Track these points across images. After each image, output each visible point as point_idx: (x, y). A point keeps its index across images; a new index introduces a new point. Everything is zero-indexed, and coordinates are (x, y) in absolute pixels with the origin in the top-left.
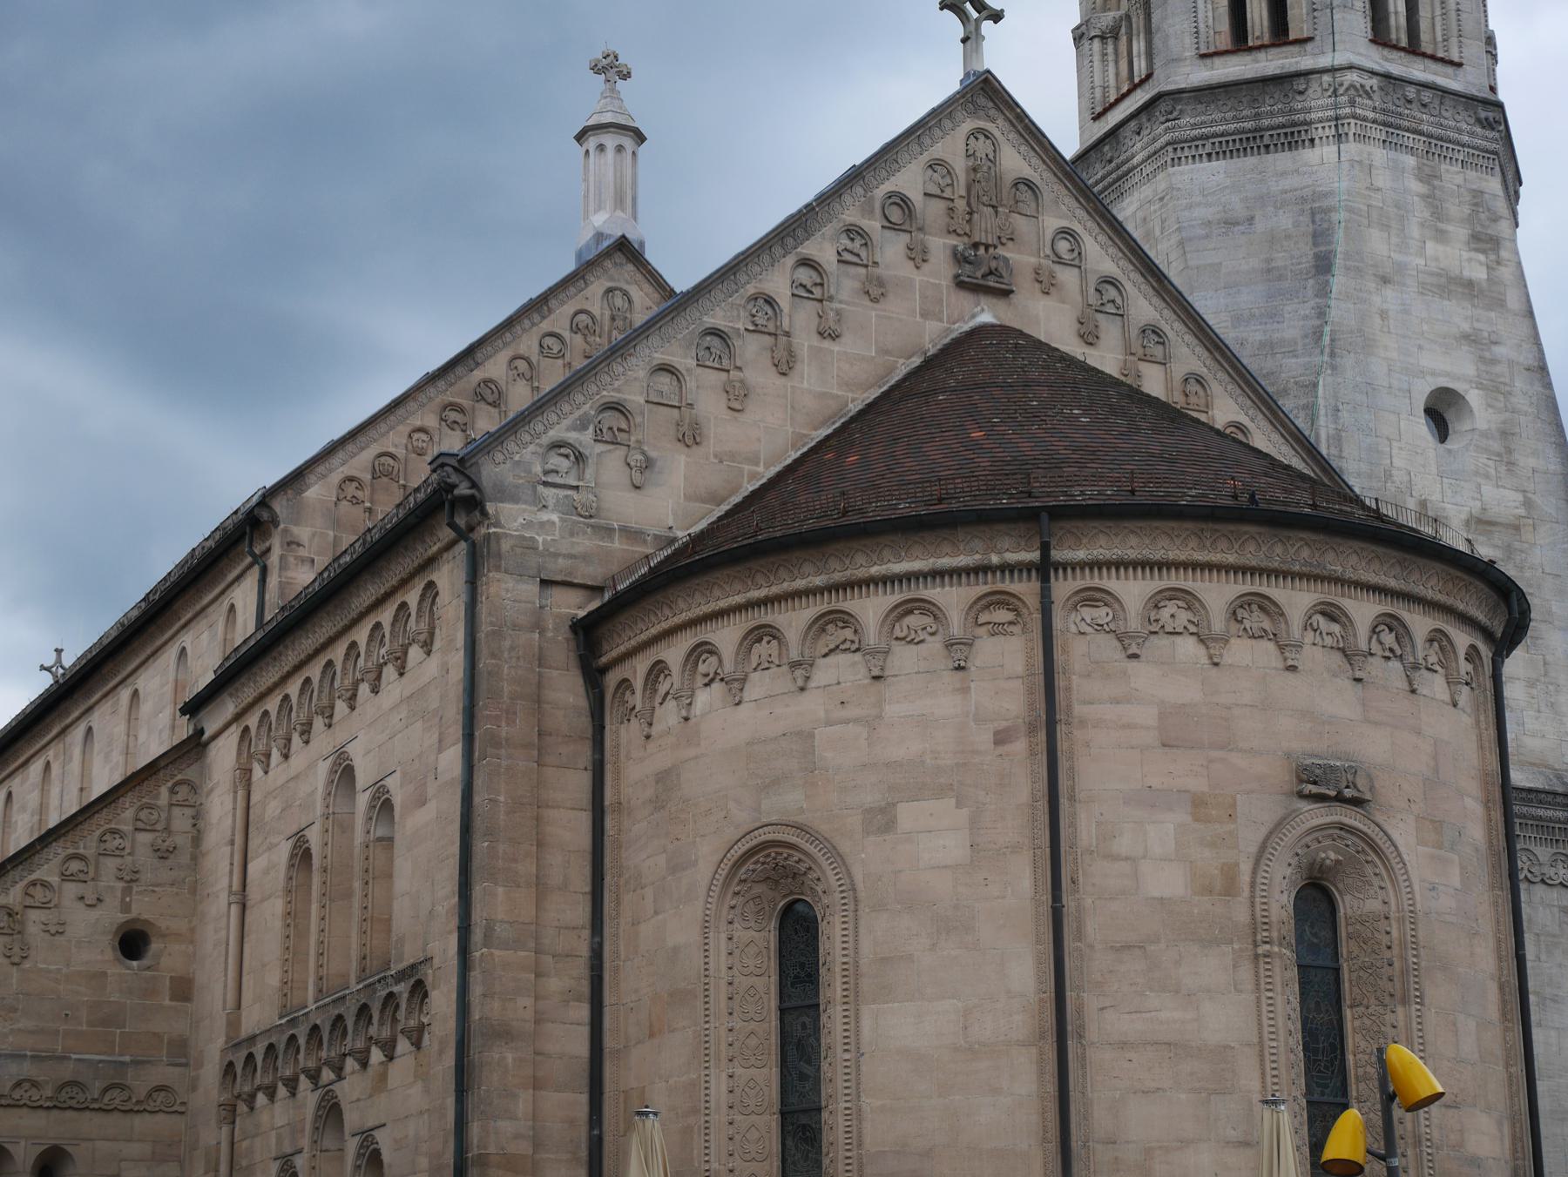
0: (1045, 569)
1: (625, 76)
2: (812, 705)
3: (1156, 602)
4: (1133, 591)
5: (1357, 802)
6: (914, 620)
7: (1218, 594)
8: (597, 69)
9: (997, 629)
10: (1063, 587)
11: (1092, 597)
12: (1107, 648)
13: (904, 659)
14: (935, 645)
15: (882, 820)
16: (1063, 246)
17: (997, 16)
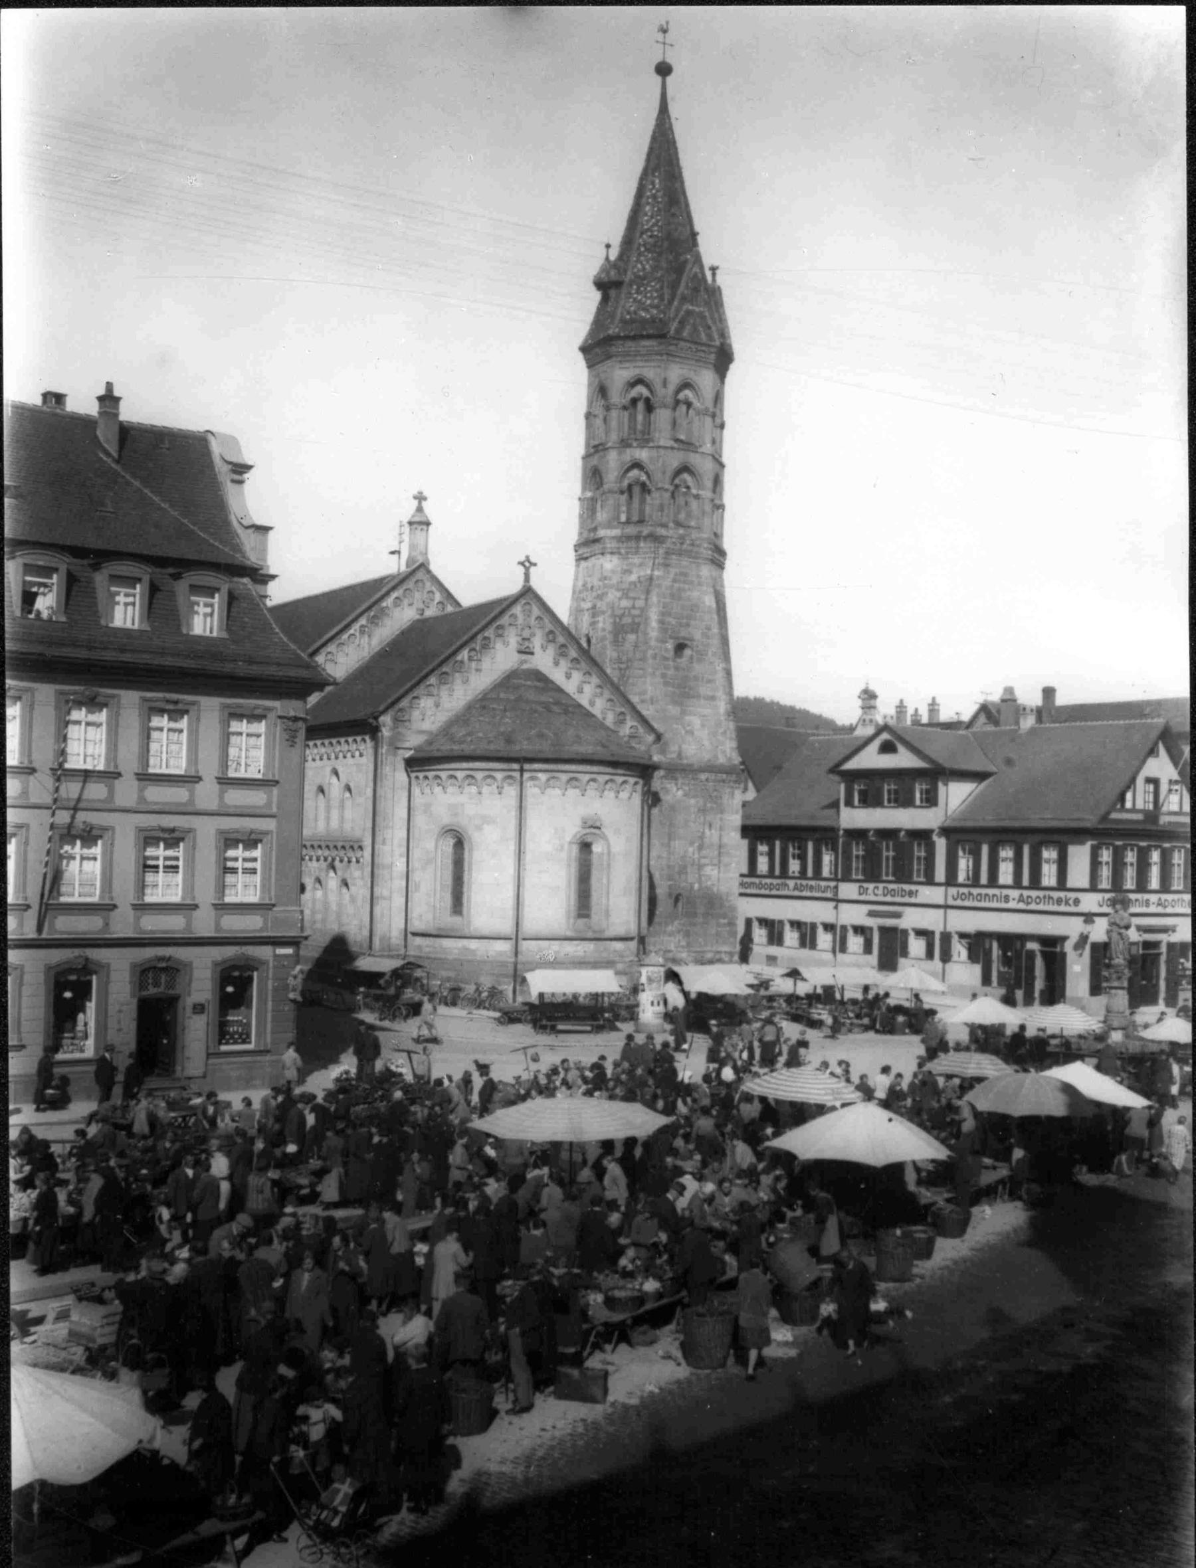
0: (522, 771)
1: (425, 499)
2: (462, 799)
3: (548, 780)
4: (543, 777)
5: (599, 828)
6: (489, 781)
7: (564, 777)
8: (415, 498)
9: (510, 785)
10: (526, 775)
11: (532, 778)
12: (536, 790)
13: (485, 790)
14: (494, 787)
15: (479, 828)
16: (551, 637)
17: (535, 565)
